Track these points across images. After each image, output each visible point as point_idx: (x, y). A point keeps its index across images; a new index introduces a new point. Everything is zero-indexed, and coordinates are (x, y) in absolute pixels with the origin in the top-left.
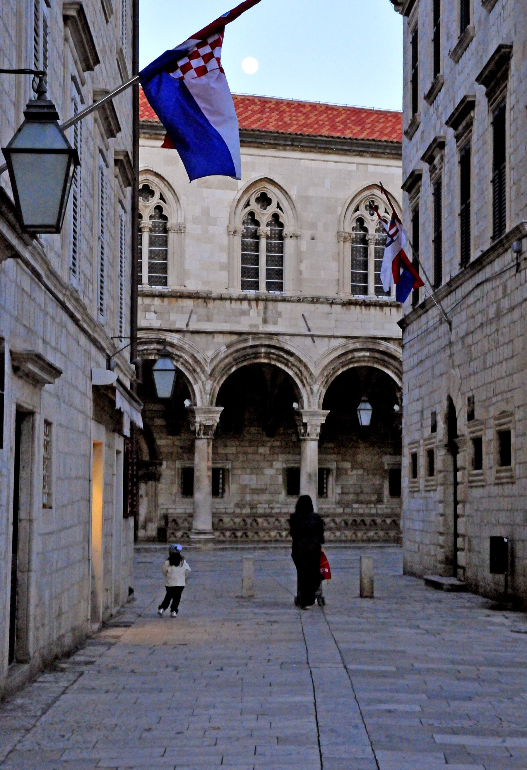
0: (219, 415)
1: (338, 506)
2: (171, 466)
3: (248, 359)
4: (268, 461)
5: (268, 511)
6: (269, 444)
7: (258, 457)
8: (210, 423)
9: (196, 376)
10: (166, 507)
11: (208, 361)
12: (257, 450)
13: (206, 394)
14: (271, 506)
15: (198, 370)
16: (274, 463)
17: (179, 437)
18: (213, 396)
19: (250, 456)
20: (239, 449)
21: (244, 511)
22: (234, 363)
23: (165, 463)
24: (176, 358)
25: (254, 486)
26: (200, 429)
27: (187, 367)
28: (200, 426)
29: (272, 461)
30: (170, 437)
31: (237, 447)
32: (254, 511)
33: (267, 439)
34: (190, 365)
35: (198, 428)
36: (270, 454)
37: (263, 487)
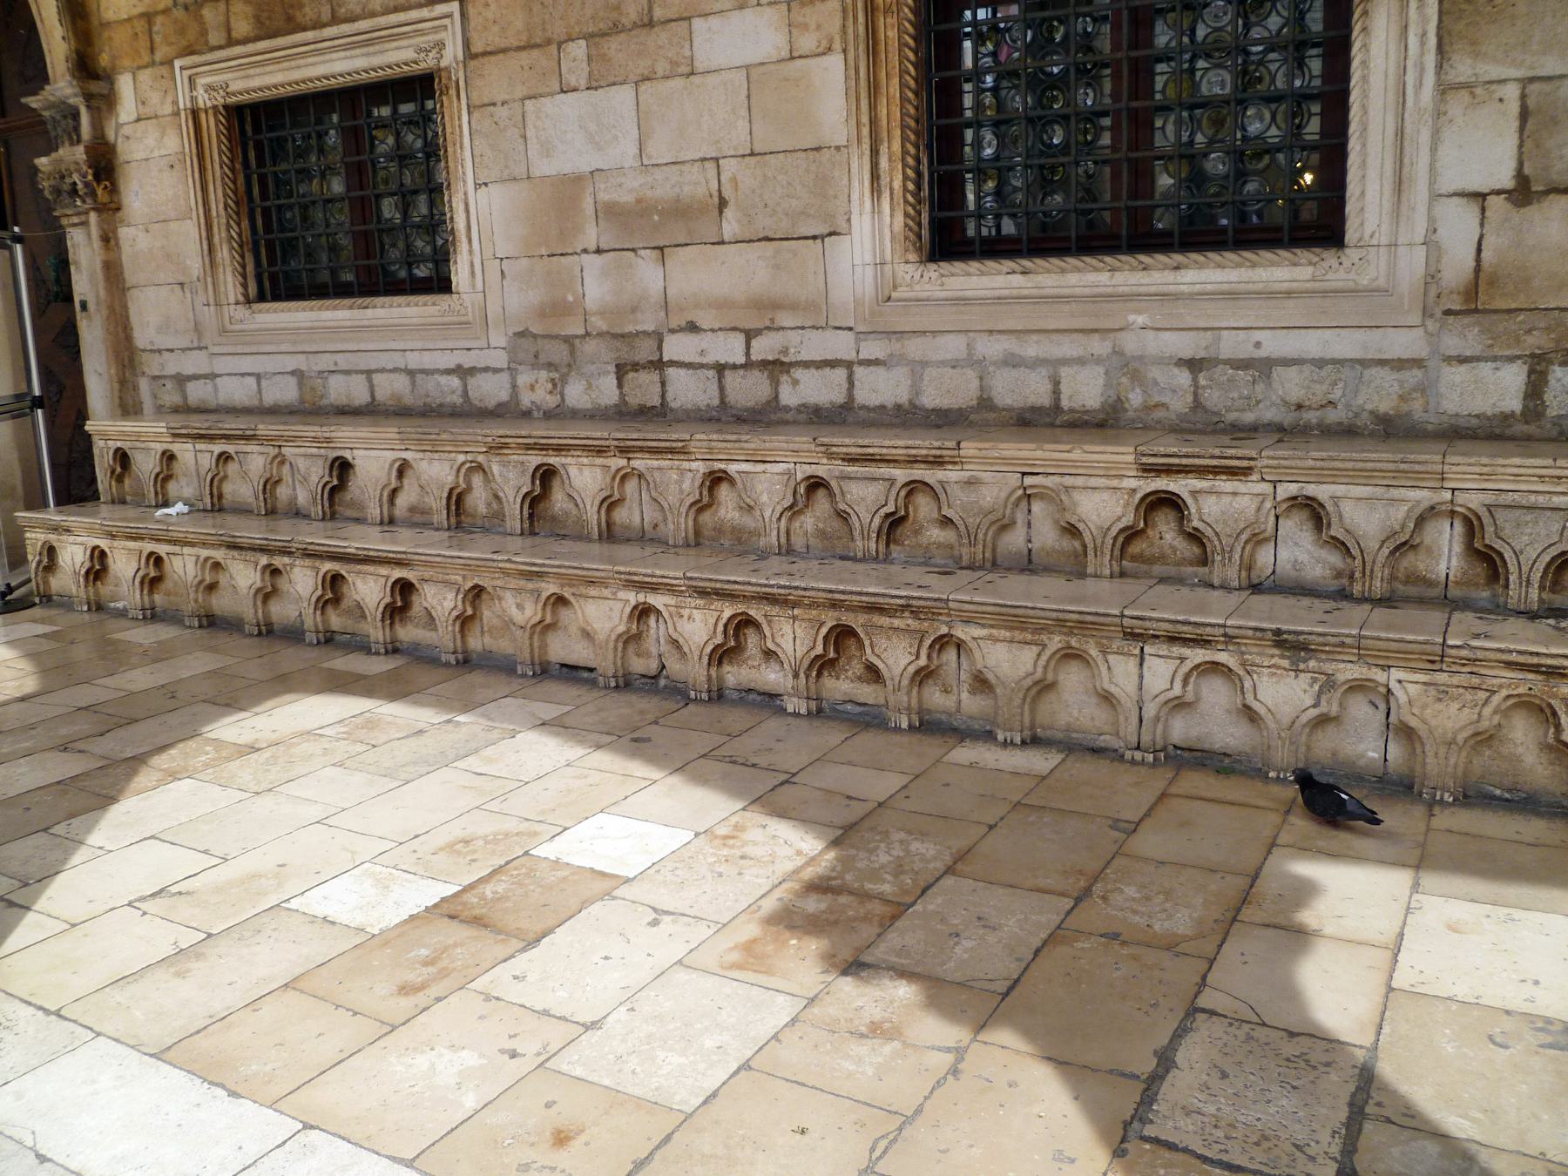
1: (1464, 338)
2: (154, 98)
5: (748, 390)
10: (173, 365)
14: (764, 347)
21: (576, 394)
25: (624, 191)
32: (644, 389)
37: (696, 185)
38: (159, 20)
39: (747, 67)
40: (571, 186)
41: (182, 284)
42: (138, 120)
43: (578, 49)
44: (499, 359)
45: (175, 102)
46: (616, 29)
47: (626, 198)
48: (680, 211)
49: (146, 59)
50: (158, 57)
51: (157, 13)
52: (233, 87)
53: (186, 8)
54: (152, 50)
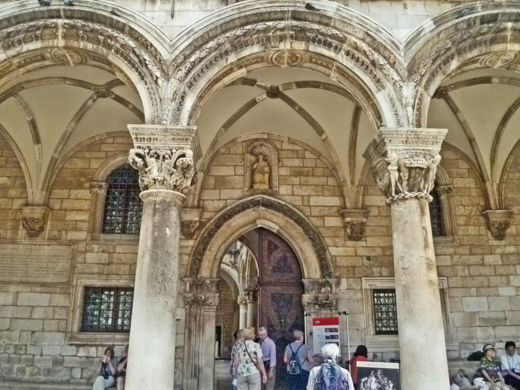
0: (438, 148)
3: (480, 44)
4: (502, 276)
6: (499, 251)
7: (485, 271)
8: (422, 163)
9: (379, 74)
11: (402, 47)
12: (483, 260)
13: (405, 106)
15: (382, 61)
16: (512, 278)
17: (363, 243)
18: (419, 110)
19: (474, 270)
20: (456, 258)
22: (453, 50)
23: (344, 281)
24: (335, 43)
25: (485, 316)
26: (400, 178)
27: (358, 60)
28: (399, 170)
29: (507, 276)
30: (350, 243)
31: (452, 256)
33: (495, 243)
34: (365, 53)
35: (394, 176)
36: (503, 265)
37: (501, 315)
38: (357, 268)
39: (509, 296)
40: (473, 315)
41: (358, 330)
42: (347, 289)
43: (474, 289)
44: (457, 348)
45: (361, 287)
46: (482, 287)
47: (485, 316)
48: (498, 320)
49: (352, 276)
50: (356, 276)
51: (357, 267)
52: (378, 285)
53: (367, 267)
54: (354, 274)
